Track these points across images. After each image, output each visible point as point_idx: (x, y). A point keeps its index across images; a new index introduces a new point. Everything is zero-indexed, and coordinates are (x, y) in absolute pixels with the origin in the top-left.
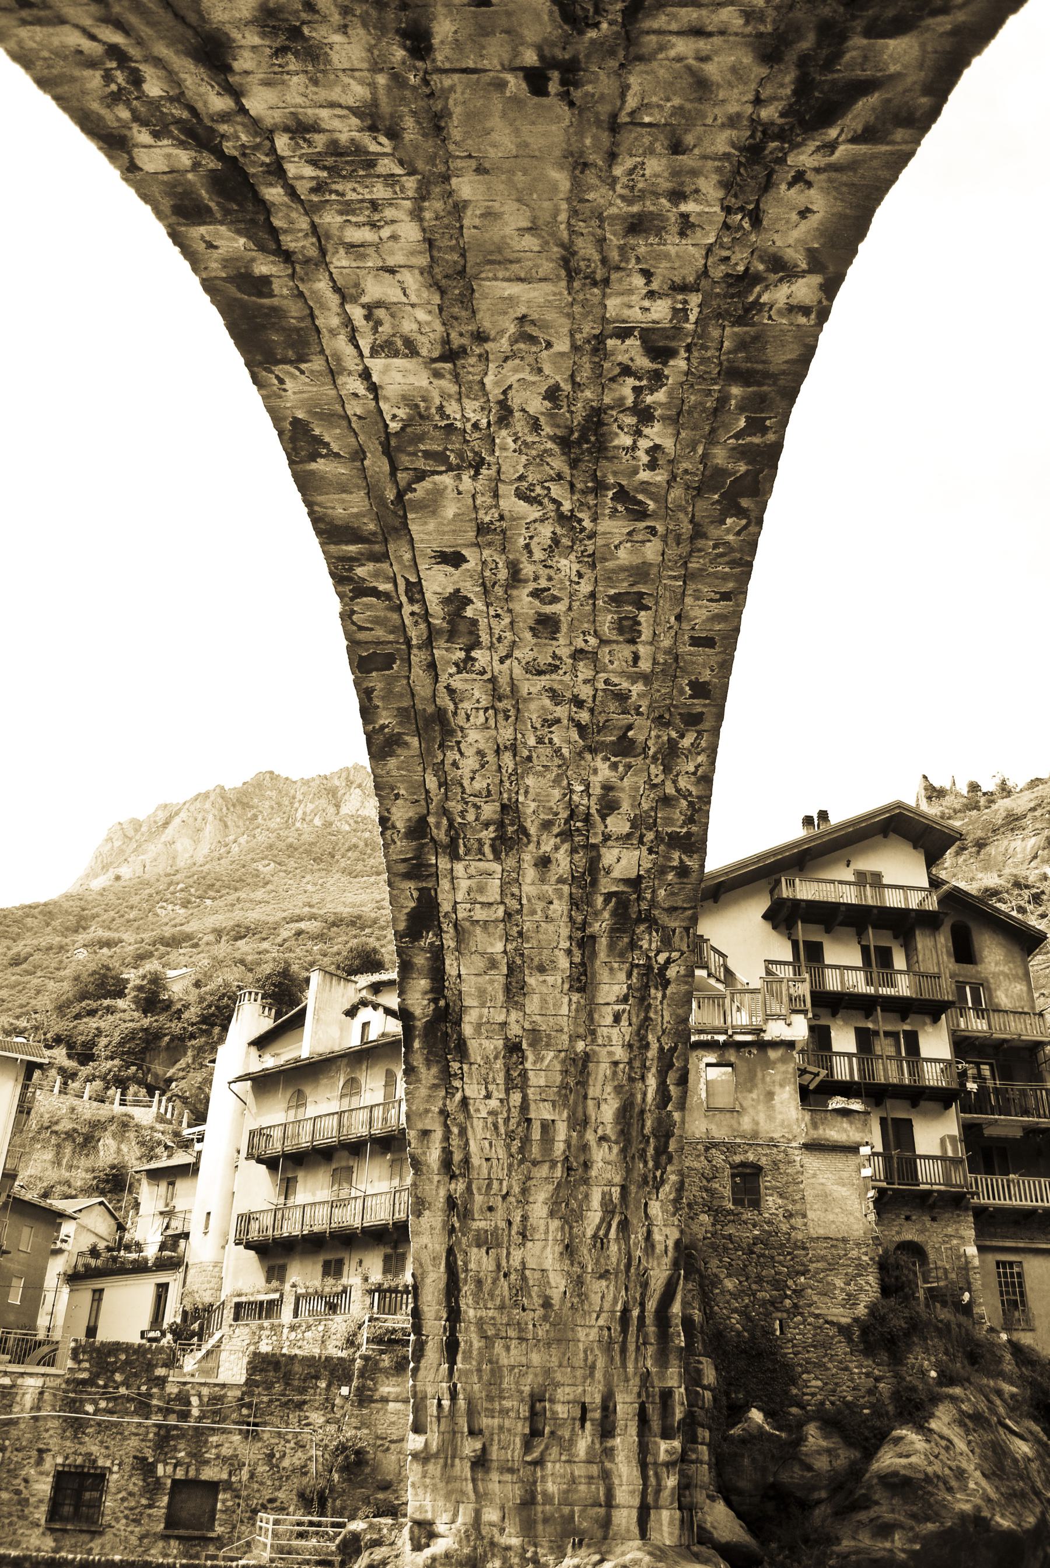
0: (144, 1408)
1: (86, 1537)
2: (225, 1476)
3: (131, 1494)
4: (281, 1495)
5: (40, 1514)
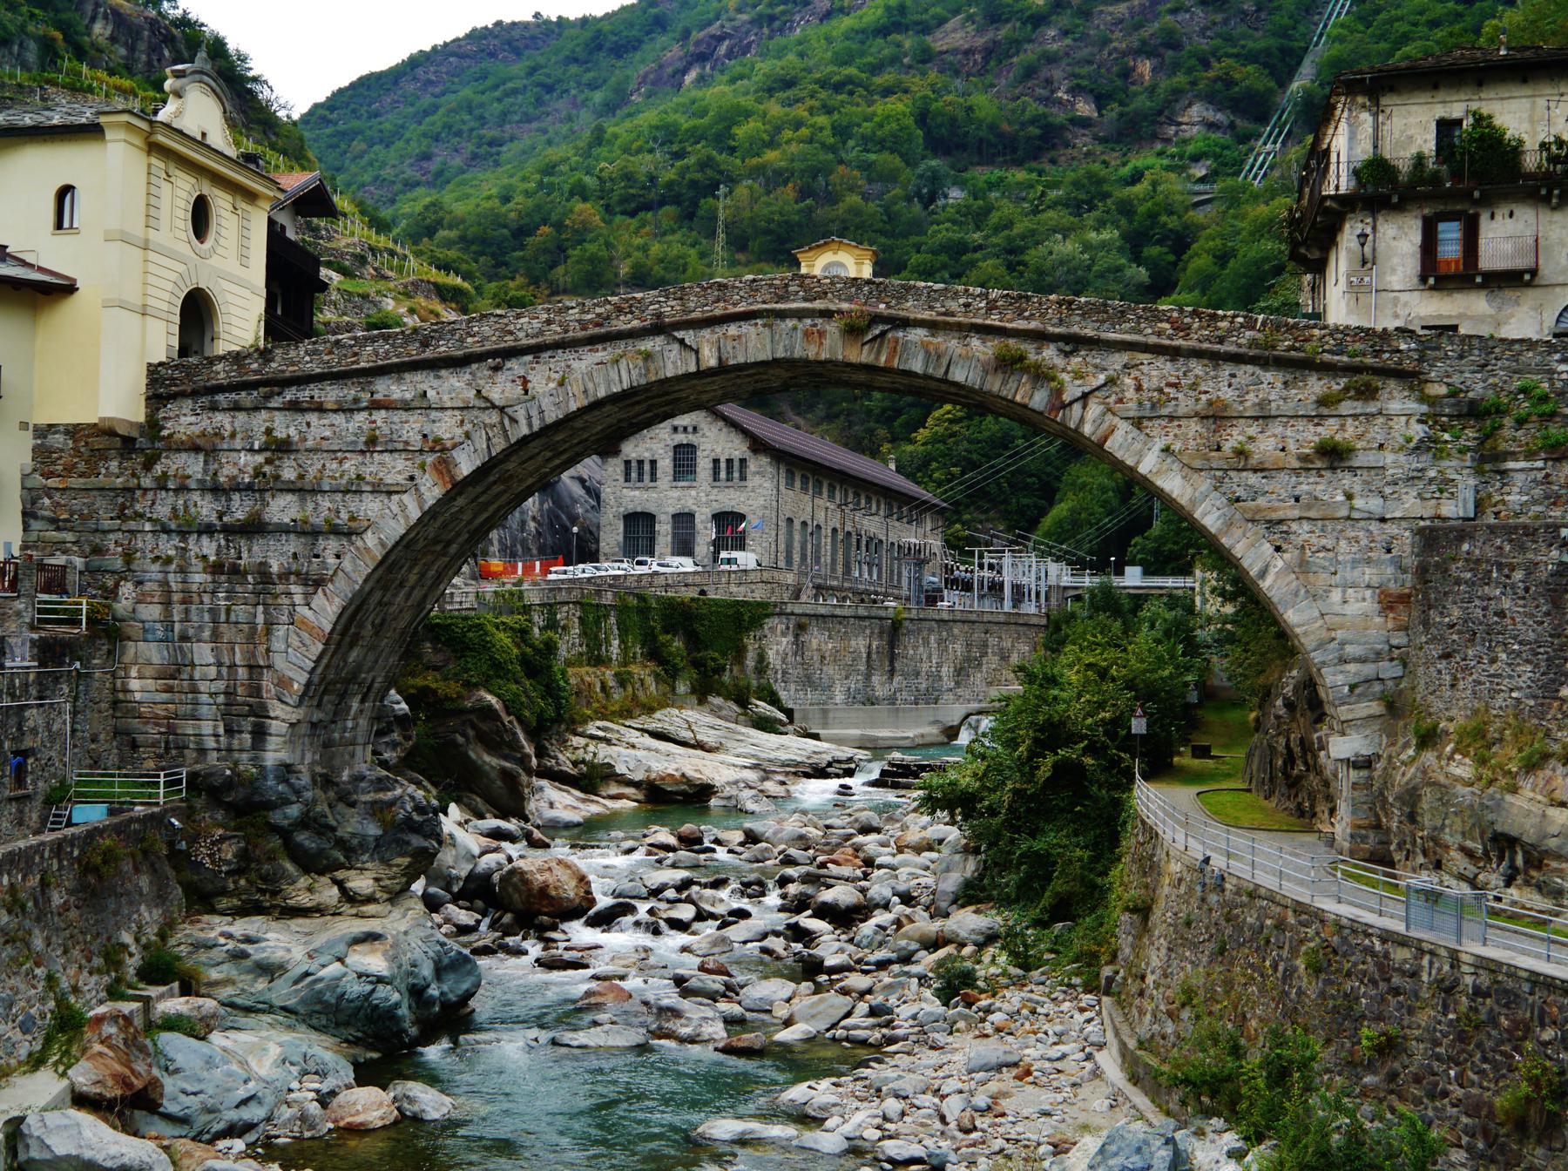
4: (53, 754)
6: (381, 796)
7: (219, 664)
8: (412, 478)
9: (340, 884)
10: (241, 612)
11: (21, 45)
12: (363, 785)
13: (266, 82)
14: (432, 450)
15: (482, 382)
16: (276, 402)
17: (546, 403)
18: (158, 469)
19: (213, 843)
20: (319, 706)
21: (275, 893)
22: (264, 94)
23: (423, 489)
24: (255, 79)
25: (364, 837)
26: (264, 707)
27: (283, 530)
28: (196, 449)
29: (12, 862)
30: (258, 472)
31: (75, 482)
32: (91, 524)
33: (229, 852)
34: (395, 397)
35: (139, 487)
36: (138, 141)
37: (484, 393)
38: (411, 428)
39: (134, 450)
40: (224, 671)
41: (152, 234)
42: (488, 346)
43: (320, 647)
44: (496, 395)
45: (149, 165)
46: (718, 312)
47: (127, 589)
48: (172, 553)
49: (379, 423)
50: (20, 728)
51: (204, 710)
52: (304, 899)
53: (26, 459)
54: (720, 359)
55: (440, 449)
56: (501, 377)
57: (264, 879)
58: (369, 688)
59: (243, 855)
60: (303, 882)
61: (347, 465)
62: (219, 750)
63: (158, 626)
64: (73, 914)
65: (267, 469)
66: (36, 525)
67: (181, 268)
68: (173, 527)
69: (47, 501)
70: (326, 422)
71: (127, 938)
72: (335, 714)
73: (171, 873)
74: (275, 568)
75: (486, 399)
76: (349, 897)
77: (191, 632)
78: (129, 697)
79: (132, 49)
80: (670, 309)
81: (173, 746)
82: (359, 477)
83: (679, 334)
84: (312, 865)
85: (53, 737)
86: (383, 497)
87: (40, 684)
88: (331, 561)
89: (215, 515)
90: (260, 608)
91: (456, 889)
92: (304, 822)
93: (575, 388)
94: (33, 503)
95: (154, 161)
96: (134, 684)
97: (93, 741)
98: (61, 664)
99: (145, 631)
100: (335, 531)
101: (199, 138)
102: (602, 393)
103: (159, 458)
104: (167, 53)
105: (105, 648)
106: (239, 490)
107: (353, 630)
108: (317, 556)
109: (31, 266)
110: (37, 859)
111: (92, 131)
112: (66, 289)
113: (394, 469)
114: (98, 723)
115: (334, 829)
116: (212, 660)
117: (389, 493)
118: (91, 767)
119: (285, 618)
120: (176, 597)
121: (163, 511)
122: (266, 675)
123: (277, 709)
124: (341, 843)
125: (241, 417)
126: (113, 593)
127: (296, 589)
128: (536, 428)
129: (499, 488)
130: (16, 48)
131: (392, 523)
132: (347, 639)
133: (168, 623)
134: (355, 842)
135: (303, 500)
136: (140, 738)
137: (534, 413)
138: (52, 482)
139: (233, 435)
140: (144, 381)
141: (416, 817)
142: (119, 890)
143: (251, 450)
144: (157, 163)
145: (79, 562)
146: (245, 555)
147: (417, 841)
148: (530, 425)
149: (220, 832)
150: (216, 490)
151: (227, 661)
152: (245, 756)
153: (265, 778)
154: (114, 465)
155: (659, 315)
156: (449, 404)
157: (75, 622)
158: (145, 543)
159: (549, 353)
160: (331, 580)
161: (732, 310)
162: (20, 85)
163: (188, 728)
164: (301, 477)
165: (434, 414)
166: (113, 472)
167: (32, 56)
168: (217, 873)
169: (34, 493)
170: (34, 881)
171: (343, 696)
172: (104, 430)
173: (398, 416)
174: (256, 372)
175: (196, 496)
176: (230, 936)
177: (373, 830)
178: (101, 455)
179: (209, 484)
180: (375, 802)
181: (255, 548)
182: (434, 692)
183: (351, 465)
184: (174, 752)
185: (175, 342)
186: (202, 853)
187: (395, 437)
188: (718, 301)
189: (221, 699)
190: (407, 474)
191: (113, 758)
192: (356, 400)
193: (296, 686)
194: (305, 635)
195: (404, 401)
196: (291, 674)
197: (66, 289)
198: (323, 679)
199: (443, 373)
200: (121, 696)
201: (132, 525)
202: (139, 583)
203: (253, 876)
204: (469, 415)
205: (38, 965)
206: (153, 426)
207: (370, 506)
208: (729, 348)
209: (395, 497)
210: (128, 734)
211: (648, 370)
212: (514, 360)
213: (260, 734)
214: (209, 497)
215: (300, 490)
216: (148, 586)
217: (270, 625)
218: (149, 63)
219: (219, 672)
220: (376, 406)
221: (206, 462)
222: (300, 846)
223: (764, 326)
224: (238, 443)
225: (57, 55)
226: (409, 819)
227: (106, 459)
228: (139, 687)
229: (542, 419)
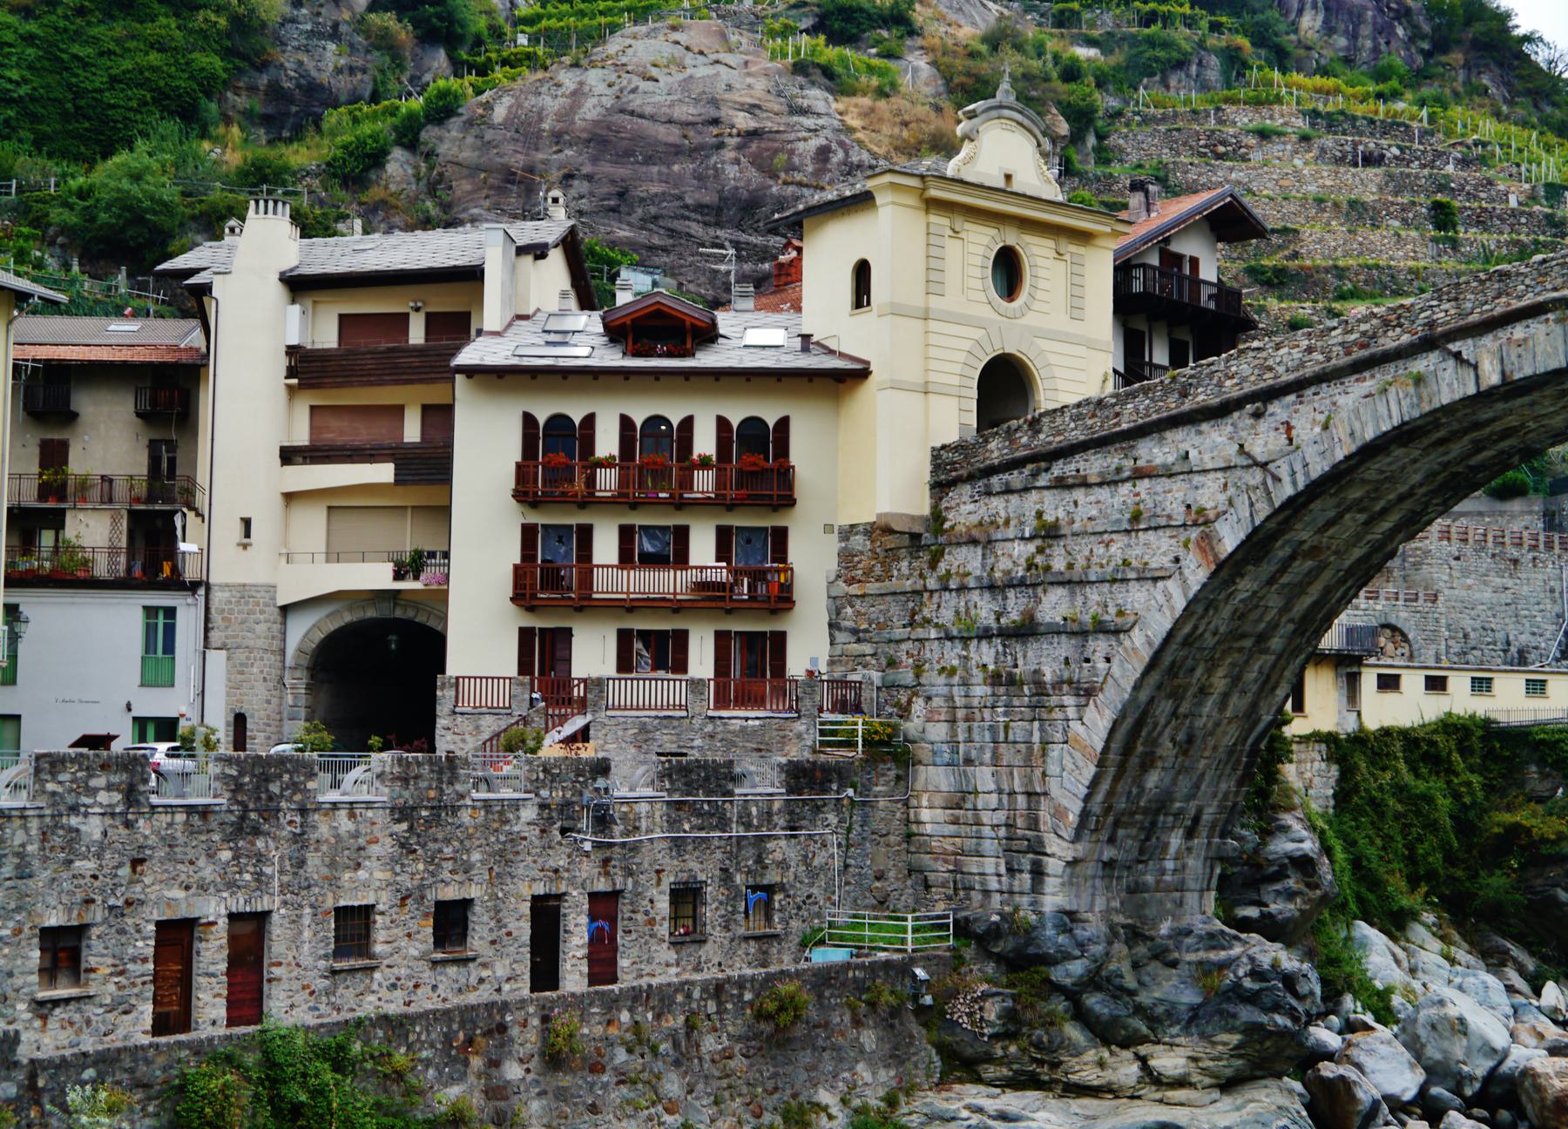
0: (723, 824)
1: (692, 948)
2: (778, 879)
3: (721, 903)
4: (815, 891)
5: (663, 930)
6: (1213, 956)
7: (1000, 792)
8: (1177, 560)
9: (1143, 1060)
10: (1018, 730)
11: (1200, 64)
12: (1189, 941)
13: (1541, 39)
14: (1195, 524)
15: (1243, 434)
16: (1043, 480)
17: (1310, 453)
18: (942, 567)
19: (975, 1000)
20: (1112, 840)
21: (1055, 1065)
22: (1540, 56)
23: (1186, 572)
24: (1528, 39)
25: (1173, 1004)
26: (1040, 842)
27: (1056, 631)
28: (974, 542)
29: (635, 999)
30: (1030, 565)
31: (872, 587)
32: (886, 635)
33: (992, 1010)
34: (1158, 461)
35: (926, 590)
36: (912, 200)
37: (1247, 449)
38: (1172, 498)
39: (920, 548)
40: (1005, 798)
41: (934, 302)
42: (1248, 388)
43: (1090, 771)
44: (1258, 450)
45: (928, 224)
46: (1499, 311)
47: (918, 706)
48: (955, 662)
49: (1143, 496)
50: (759, 860)
51: (989, 846)
52: (1090, 1076)
53: (832, 564)
54: (1503, 373)
55: (1201, 520)
56: (1264, 425)
57: (1038, 1046)
58: (1196, 820)
59: (1009, 1016)
60: (1091, 1055)
61: (1113, 549)
62: (1002, 892)
63: (945, 747)
64: (739, 1063)
65: (1039, 560)
66: (841, 637)
67: (978, 334)
68: (955, 633)
69: (849, 610)
70: (1092, 498)
71: (825, 1097)
72: (1141, 851)
73: (915, 1028)
74: (1048, 678)
75: (1249, 455)
76: (1152, 1077)
77: (974, 754)
78: (922, 829)
79: (1354, 37)
80: (1445, 314)
81: (961, 886)
82: (1126, 563)
83: (1454, 347)
84: (1108, 1034)
85: (813, 874)
86: (1149, 584)
87: (791, 813)
88: (1101, 665)
89: (993, 617)
90: (1036, 724)
91: (1468, 1092)
92: (1095, 980)
93: (1340, 431)
94: (838, 614)
95: (934, 219)
96: (925, 815)
97: (878, 878)
98: (825, 791)
99: (934, 753)
100: (1101, 628)
101: (1001, 184)
102: (1370, 434)
103: (942, 554)
104: (1400, 31)
105: (892, 774)
106: (1014, 586)
107: (1140, 749)
108: (1087, 660)
109: (831, 352)
110: (680, 998)
111: (864, 200)
112: (861, 374)
113: (1157, 549)
114: (887, 858)
115: (1132, 993)
116: (992, 787)
117: (1155, 579)
118: (874, 908)
119: (1059, 737)
120: (960, 714)
121: (947, 616)
122: (1044, 804)
123: (1053, 845)
124: (1139, 1010)
125: (1014, 499)
126: (905, 711)
127: (1069, 700)
128: (1301, 486)
129: (1303, 566)
130: (1194, 68)
131: (1158, 616)
132: (1134, 760)
133: (953, 743)
134: (1160, 1010)
135: (1073, 594)
136: (931, 877)
137: (1298, 467)
138: (854, 589)
139: (1007, 522)
140: (928, 468)
141: (1248, 983)
142: (820, 1042)
143: (1023, 539)
144: (940, 221)
145: (876, 676)
146: (1020, 662)
147: (1247, 1014)
148: (1294, 483)
149: (985, 987)
150: (992, 588)
151: (1006, 787)
152: (1025, 900)
153: (1043, 927)
154: (904, 564)
155: (1431, 324)
156: (1210, 466)
157: (850, 744)
158: (932, 651)
159: (1313, 389)
160: (1101, 689)
161: (1517, 304)
162: (1194, 112)
163: (972, 865)
164: (1070, 566)
165: (1197, 479)
166: (905, 574)
167: (1213, 74)
168: (976, 1037)
169: (838, 602)
170: (676, 1021)
171: (1150, 830)
172: (881, 530)
173: (1161, 484)
174: (1026, 446)
175: (975, 596)
176: (979, 1110)
177: (1189, 997)
178: (892, 555)
179: (985, 582)
180: (1200, 963)
181: (1030, 654)
182: (1528, 831)
183: (1118, 548)
184: (962, 893)
185: (972, 420)
186: (960, 1011)
187: (1158, 510)
188: (1498, 296)
189: (1002, 832)
190: (1171, 557)
191: (907, 898)
192: (1119, 470)
193: (1071, 817)
194: (1078, 755)
195: (1165, 466)
196: (1065, 802)
197: (861, 374)
198: (1108, 809)
199: (1205, 427)
200: (914, 828)
201: (920, 633)
202: (929, 698)
203: (1025, 1043)
204: (1233, 476)
205: (668, 1111)
206: (937, 517)
207: (1136, 597)
208: (1514, 358)
209: (1160, 584)
210: (921, 872)
211: (1420, 398)
212: (1276, 402)
213: (1038, 873)
214: (987, 595)
215: (1069, 582)
216: (937, 702)
217: (1045, 743)
218: (1376, 50)
219: (1000, 800)
220: (1139, 474)
221: (984, 555)
222: (1090, 1010)
223: (1557, 321)
224: (1011, 533)
225: (1245, 65)
226: (1237, 985)
227: (898, 560)
228: (931, 817)
229: (1307, 474)
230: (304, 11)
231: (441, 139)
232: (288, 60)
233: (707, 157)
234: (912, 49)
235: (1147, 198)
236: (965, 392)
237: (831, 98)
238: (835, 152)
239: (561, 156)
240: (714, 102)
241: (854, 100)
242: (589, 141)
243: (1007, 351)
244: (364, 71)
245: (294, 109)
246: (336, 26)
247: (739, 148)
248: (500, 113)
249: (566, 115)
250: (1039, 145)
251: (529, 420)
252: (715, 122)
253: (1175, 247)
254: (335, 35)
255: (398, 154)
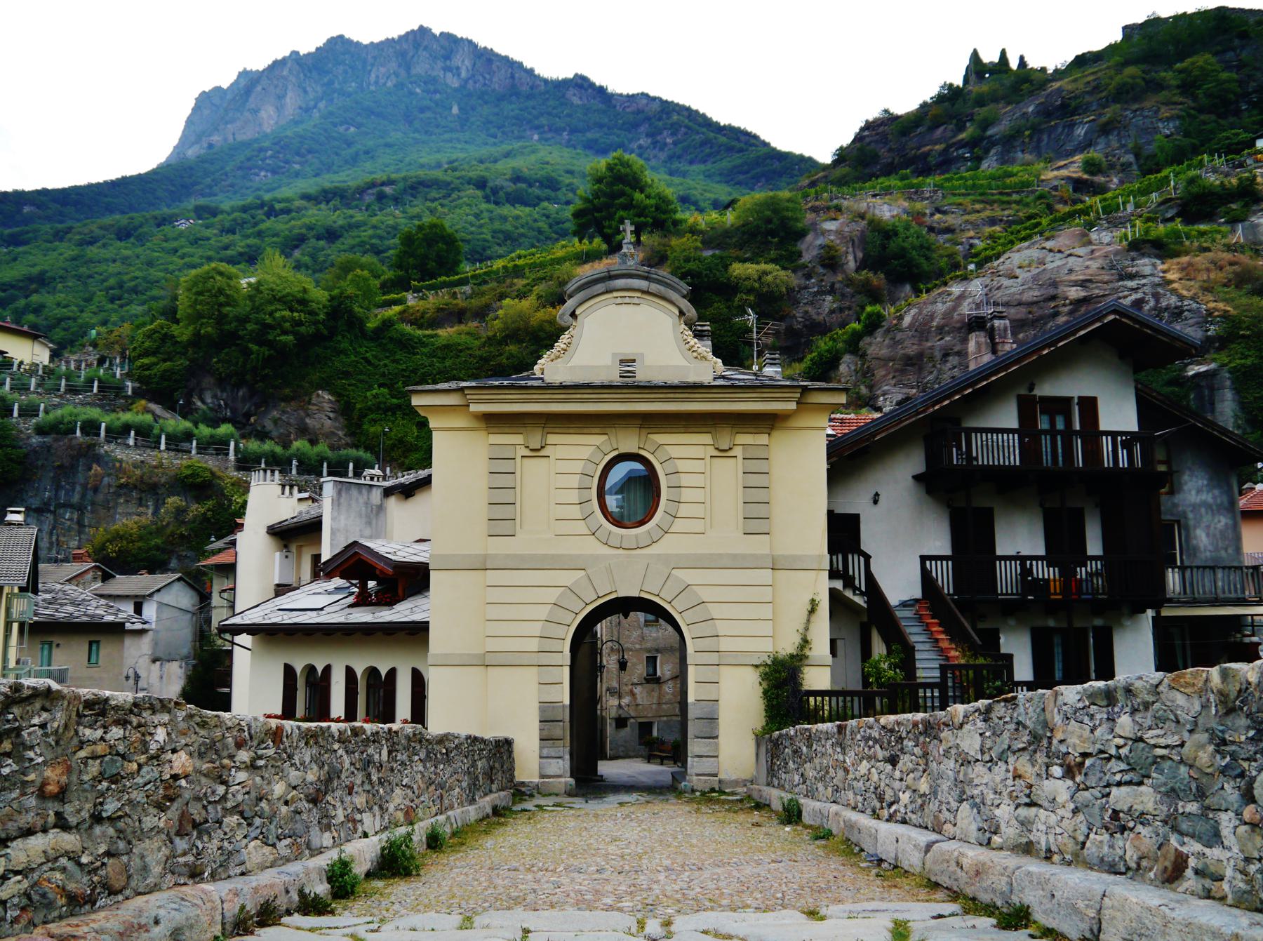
36: (459, 421)
101: (613, 376)
144: (513, 440)
230: (813, 281)
231: (870, 344)
232: (798, 314)
233: (1046, 324)
234: (1255, 213)
235: (992, 338)
236: (546, 659)
237: (1158, 262)
238: (1147, 302)
239: (942, 342)
240: (1054, 284)
241: (1175, 260)
242: (961, 328)
243: (622, 594)
244: (849, 308)
245: (803, 340)
246: (832, 285)
247: (1071, 313)
248: (907, 320)
249: (948, 314)
250: (682, 313)
251: (289, 671)
252: (1054, 298)
253: (1049, 388)
254: (832, 291)
255: (847, 358)
